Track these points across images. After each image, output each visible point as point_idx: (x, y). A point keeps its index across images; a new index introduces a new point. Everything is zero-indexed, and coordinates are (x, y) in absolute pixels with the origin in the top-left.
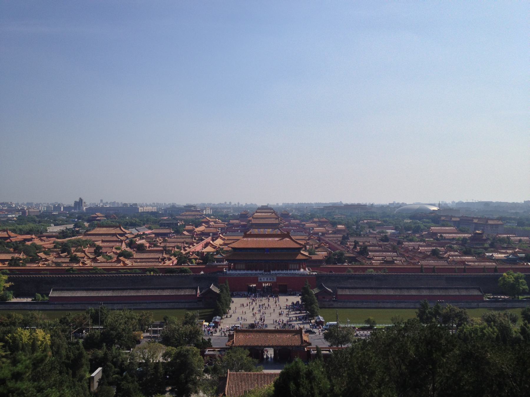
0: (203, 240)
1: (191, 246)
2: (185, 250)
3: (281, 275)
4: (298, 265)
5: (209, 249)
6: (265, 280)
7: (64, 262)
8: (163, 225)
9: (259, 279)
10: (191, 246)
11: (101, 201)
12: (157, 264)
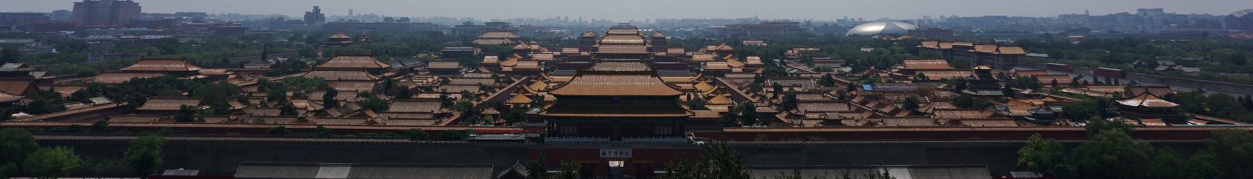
2: (479, 100)
3: (641, 146)
6: (613, 155)
7: (272, 117)
8: (448, 56)
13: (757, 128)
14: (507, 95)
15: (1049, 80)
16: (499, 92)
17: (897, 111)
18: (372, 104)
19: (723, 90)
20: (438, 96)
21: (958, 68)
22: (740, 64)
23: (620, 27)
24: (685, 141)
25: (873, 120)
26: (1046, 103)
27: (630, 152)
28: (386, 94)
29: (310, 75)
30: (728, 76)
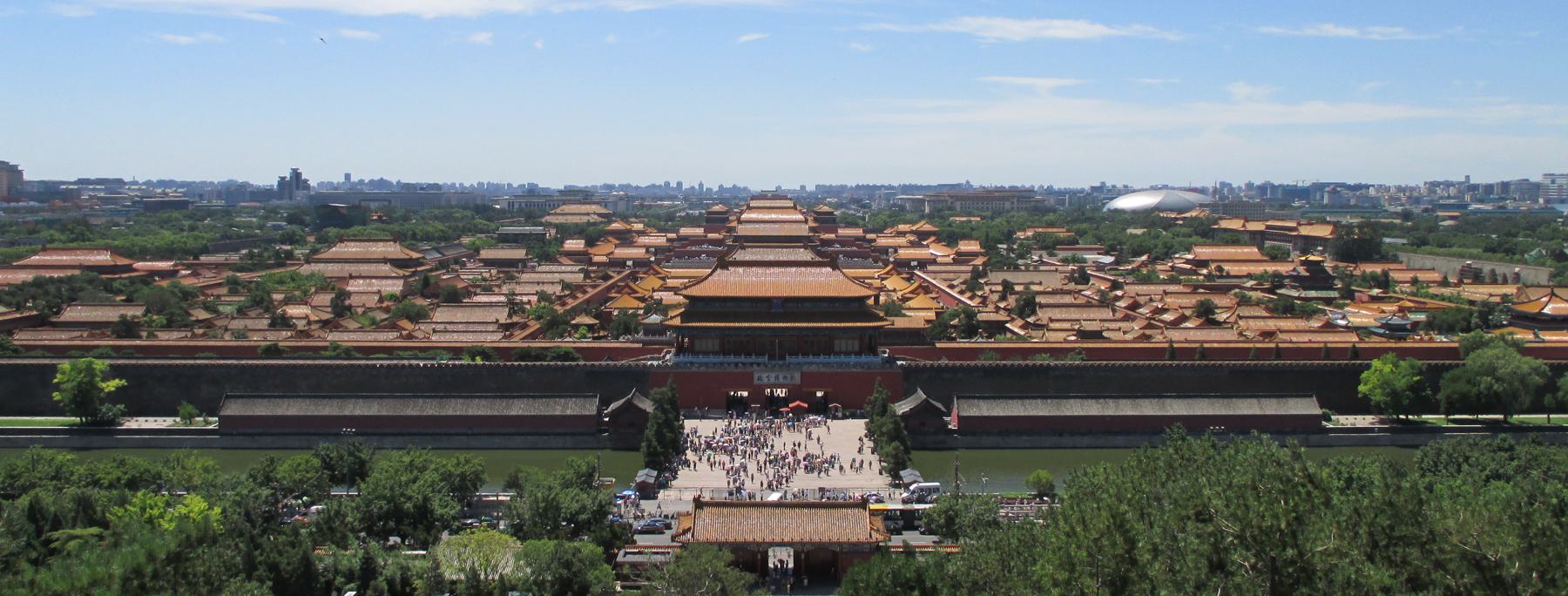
0: (606, 278)
2: (564, 304)
3: (813, 368)
4: (857, 344)
6: (772, 380)
8: (507, 240)
9: (756, 376)
11: (348, 176)
12: (490, 337)
13: (979, 342)
14: (604, 298)
15: (1409, 276)
16: (591, 292)
17: (1184, 318)
18: (401, 311)
19: (926, 289)
20: (503, 299)
21: (1274, 258)
22: (948, 251)
23: (763, 196)
24: (878, 360)
25: (1148, 332)
26: (1402, 309)
27: (797, 376)
28: (425, 296)
29: (306, 269)
30: (930, 268)
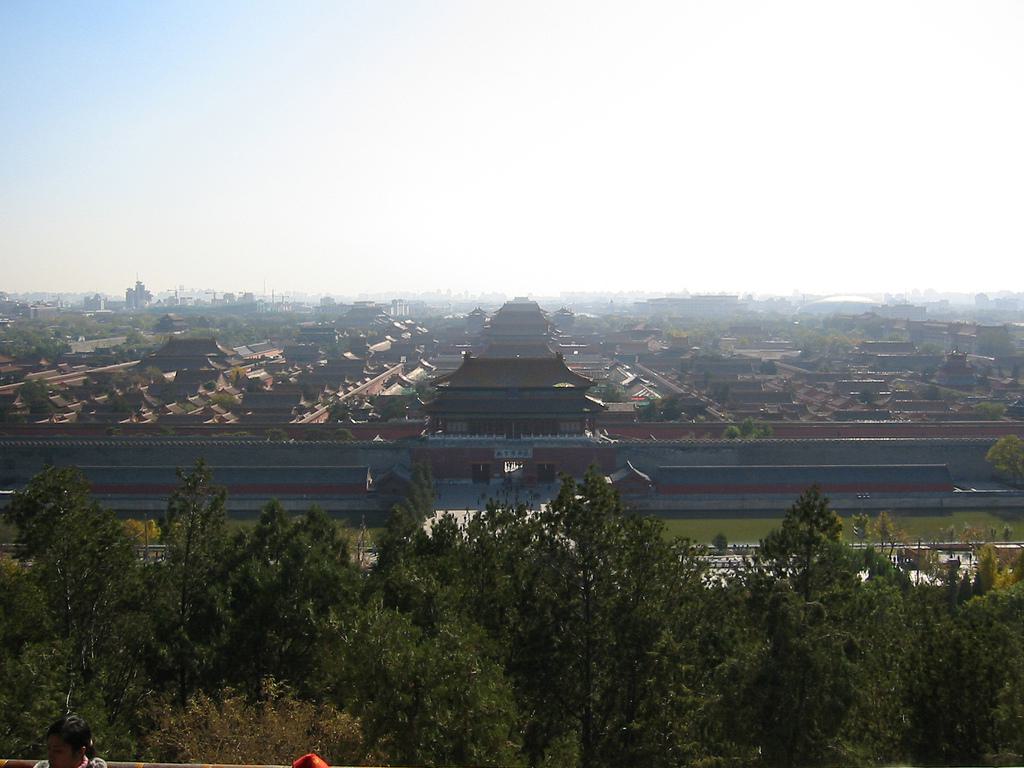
1: (359, 384)
5: (395, 389)
10: (359, 384)
27: (530, 451)
